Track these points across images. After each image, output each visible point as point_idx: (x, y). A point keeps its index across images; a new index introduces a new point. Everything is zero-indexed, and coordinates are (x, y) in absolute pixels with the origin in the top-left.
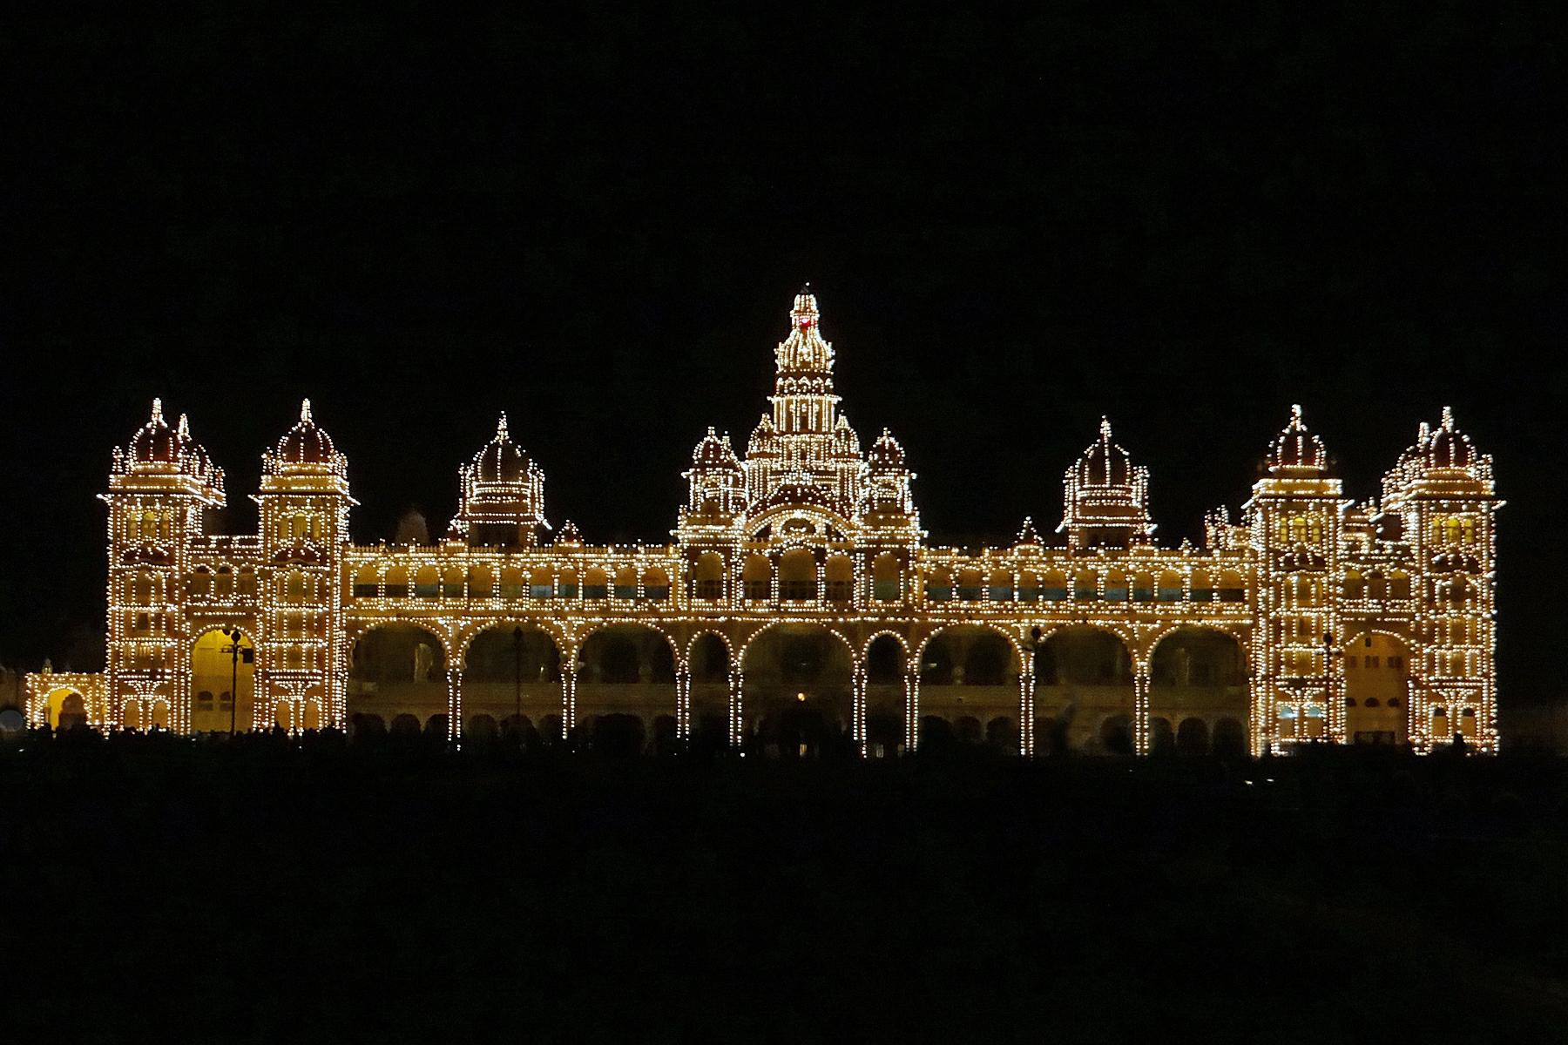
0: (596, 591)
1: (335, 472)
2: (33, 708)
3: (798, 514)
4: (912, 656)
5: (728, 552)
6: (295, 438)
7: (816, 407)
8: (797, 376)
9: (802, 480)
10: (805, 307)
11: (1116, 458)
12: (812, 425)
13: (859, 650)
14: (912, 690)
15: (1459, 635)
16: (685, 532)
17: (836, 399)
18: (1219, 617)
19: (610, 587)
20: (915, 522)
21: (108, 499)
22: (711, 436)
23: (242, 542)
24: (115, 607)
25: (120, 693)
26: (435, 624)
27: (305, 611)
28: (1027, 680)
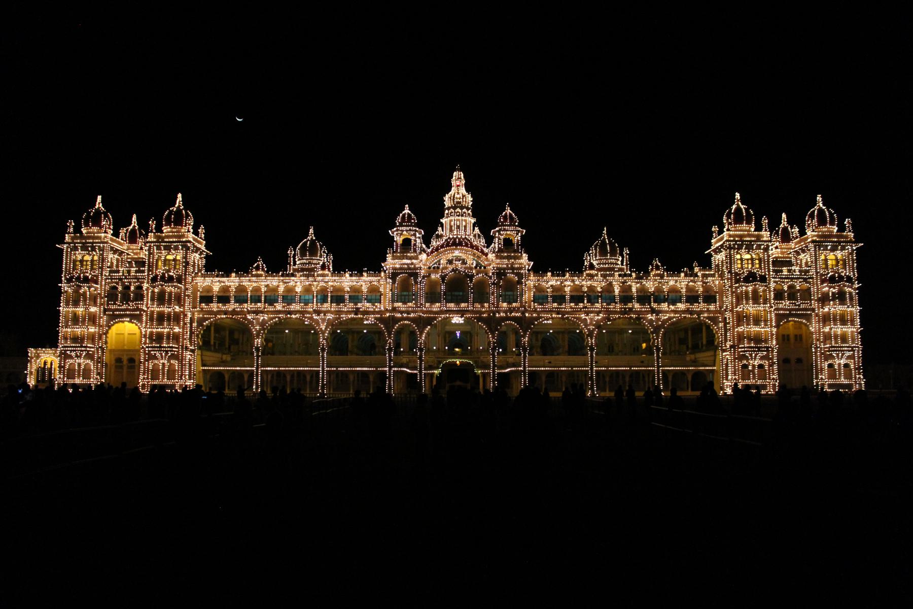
2: (31, 368)
3: (457, 253)
4: (524, 337)
5: (416, 275)
6: (171, 213)
7: (464, 223)
8: (455, 208)
9: (459, 236)
10: (458, 179)
13: (493, 334)
14: (525, 357)
15: (844, 322)
16: (391, 262)
17: (473, 220)
19: (347, 296)
20: (525, 256)
22: (407, 211)
25: (65, 359)
27: (167, 310)
28: (592, 350)
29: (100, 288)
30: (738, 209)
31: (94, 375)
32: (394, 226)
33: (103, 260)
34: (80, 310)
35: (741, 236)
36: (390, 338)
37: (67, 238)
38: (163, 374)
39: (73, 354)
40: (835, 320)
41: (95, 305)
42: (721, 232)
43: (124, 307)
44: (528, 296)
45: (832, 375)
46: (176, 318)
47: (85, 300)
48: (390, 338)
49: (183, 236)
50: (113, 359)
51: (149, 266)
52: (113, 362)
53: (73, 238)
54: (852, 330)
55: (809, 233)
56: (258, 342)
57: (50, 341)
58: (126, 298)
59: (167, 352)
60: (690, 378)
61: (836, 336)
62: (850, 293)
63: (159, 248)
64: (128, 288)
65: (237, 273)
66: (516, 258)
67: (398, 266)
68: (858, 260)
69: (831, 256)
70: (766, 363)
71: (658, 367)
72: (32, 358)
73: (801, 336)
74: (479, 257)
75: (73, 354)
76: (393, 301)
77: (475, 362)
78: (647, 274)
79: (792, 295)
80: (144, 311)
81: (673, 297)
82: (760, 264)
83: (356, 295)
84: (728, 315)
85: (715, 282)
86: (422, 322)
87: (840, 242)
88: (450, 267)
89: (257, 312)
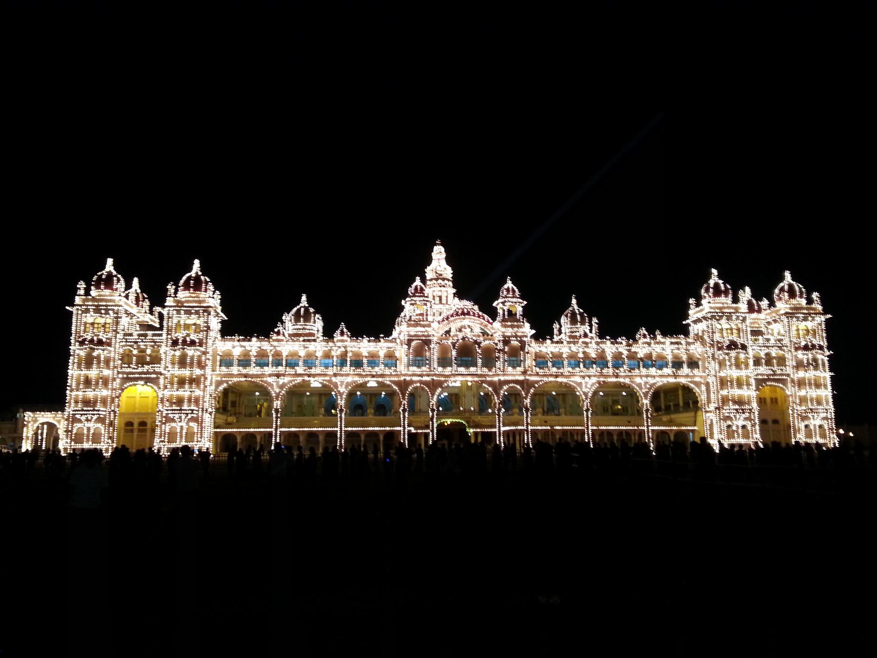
0: (357, 363)
1: (212, 298)
2: (27, 432)
7: (445, 294)
8: (437, 279)
10: (439, 253)
11: (581, 314)
12: (444, 301)
13: (498, 394)
14: (527, 416)
15: (818, 386)
17: (454, 291)
18: (685, 376)
19: (365, 361)
20: (527, 325)
21: (74, 310)
23: (154, 335)
24: (74, 372)
25: (73, 423)
26: (266, 382)
28: (587, 410)
29: (115, 351)
30: (716, 285)
31: (105, 439)
32: (407, 295)
33: (117, 323)
34: (93, 373)
35: (720, 308)
36: (404, 399)
37: (78, 300)
38: (181, 437)
39: (83, 418)
40: (810, 384)
41: (108, 367)
42: (698, 304)
43: (140, 370)
44: (529, 362)
45: (809, 435)
46: (194, 381)
47: (99, 362)
48: (404, 399)
49: (204, 301)
50: (123, 422)
51: (168, 330)
52: (123, 425)
53: (84, 301)
54: (827, 393)
55: (779, 305)
56: (277, 404)
57: (57, 403)
58: (142, 362)
59: (187, 414)
60: (672, 438)
61: (812, 400)
62: (822, 360)
63: (178, 312)
64: (143, 351)
65: (258, 337)
66: (518, 327)
67: (412, 333)
68: (828, 330)
69: (803, 325)
70: (749, 424)
71: (648, 426)
72: (29, 422)
73: (776, 399)
74: (486, 326)
75: (83, 418)
76: (409, 365)
77: (468, 422)
78: (636, 341)
79: (769, 361)
80: (161, 374)
81: (659, 363)
82: (739, 333)
83: (373, 360)
84: (711, 380)
85: (697, 349)
86: (433, 385)
87: (810, 314)
88: (460, 335)
89: (278, 376)
